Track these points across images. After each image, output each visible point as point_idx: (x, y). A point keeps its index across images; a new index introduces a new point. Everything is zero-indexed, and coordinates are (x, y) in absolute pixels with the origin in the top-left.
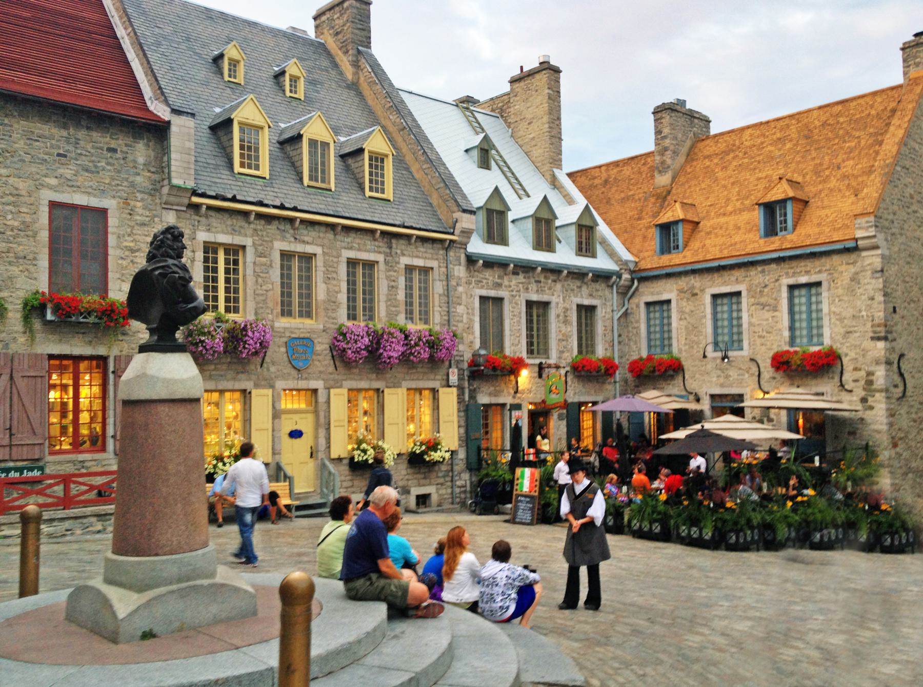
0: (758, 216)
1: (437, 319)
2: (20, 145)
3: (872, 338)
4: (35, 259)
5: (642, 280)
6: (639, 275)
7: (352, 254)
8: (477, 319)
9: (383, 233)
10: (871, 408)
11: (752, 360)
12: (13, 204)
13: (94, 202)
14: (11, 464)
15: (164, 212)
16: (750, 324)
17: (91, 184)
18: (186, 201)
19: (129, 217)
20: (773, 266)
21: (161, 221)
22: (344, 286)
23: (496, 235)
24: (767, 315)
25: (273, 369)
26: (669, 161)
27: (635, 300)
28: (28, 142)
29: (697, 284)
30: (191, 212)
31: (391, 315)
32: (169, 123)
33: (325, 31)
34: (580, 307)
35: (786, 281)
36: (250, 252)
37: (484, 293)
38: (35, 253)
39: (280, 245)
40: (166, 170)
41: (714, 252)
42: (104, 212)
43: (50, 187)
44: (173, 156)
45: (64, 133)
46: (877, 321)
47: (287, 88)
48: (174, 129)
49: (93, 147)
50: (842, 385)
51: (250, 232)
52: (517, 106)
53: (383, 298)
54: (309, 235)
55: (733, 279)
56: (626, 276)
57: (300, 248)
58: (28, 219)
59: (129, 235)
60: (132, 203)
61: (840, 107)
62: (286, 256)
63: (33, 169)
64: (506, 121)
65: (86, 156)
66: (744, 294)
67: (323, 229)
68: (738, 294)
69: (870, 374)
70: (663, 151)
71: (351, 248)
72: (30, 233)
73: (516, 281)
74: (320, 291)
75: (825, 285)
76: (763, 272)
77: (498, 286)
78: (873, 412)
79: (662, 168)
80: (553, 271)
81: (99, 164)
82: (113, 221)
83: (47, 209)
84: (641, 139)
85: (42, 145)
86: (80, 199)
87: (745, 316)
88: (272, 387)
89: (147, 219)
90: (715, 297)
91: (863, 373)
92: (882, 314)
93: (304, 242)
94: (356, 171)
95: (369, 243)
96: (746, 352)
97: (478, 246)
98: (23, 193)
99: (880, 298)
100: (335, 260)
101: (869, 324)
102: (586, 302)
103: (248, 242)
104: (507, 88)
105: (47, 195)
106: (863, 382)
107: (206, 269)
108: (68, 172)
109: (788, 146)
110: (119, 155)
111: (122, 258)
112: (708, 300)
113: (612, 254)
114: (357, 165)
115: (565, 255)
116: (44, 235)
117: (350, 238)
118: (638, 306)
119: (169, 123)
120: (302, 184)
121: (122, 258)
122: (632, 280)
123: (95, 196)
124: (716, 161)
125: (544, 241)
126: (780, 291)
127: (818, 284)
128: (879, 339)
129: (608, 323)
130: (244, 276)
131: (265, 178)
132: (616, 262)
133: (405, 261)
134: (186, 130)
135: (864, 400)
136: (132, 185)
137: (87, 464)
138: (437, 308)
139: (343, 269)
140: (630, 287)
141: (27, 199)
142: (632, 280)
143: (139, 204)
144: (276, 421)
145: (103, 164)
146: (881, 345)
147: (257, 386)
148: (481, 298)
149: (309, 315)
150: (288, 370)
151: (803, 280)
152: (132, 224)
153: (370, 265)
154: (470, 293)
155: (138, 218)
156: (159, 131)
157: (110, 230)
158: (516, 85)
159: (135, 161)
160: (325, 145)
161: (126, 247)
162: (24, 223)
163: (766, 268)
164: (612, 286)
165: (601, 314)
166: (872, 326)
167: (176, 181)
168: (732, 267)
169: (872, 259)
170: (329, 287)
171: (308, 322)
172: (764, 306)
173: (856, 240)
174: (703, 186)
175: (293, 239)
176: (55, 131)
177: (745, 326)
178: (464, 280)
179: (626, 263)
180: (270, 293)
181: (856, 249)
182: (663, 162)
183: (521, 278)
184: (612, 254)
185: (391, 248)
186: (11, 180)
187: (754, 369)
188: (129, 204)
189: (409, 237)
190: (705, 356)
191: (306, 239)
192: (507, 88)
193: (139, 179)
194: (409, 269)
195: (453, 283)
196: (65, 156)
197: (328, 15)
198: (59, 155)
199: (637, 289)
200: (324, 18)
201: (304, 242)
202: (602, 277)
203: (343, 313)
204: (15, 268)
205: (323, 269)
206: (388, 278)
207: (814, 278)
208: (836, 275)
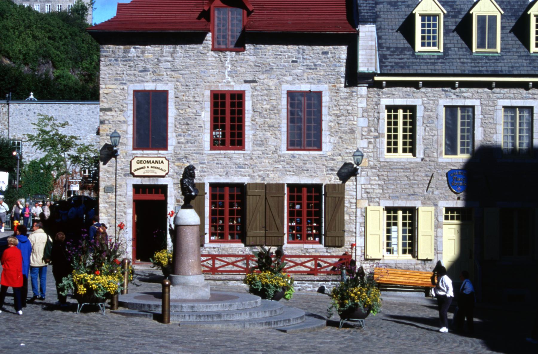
4: (279, 127)
7: (508, 103)
12: (267, 95)
13: (314, 88)
17: (312, 76)
19: (335, 94)
21: (357, 95)
25: (436, 192)
28: (275, 56)
38: (279, 123)
39: (445, 101)
42: (319, 94)
49: (313, 53)
54: (468, 92)
58: (275, 103)
59: (336, 106)
60: (338, 85)
62: (451, 110)
65: (309, 59)
72: (276, 111)
81: (317, 63)
82: (325, 99)
83: (286, 96)
85: (283, 57)
86: (305, 87)
88: (436, 205)
89: (348, 94)
100: (491, 108)
105: (287, 87)
107: (389, 123)
108: (298, 71)
110: (330, 55)
111: (331, 121)
116: (284, 113)
121: (331, 121)
123: (314, 84)
131: (439, 52)
134: (370, 34)
137: (309, 250)
141: (274, 91)
144: (439, 230)
145: (320, 63)
147: (424, 204)
155: (342, 94)
157: (323, 104)
160: (493, 19)
161: (334, 114)
162: (272, 106)
175: (454, 97)
188: (335, 86)
191: (465, 95)
196: (296, 62)
198: (293, 61)
201: (464, 97)
205: (481, 116)
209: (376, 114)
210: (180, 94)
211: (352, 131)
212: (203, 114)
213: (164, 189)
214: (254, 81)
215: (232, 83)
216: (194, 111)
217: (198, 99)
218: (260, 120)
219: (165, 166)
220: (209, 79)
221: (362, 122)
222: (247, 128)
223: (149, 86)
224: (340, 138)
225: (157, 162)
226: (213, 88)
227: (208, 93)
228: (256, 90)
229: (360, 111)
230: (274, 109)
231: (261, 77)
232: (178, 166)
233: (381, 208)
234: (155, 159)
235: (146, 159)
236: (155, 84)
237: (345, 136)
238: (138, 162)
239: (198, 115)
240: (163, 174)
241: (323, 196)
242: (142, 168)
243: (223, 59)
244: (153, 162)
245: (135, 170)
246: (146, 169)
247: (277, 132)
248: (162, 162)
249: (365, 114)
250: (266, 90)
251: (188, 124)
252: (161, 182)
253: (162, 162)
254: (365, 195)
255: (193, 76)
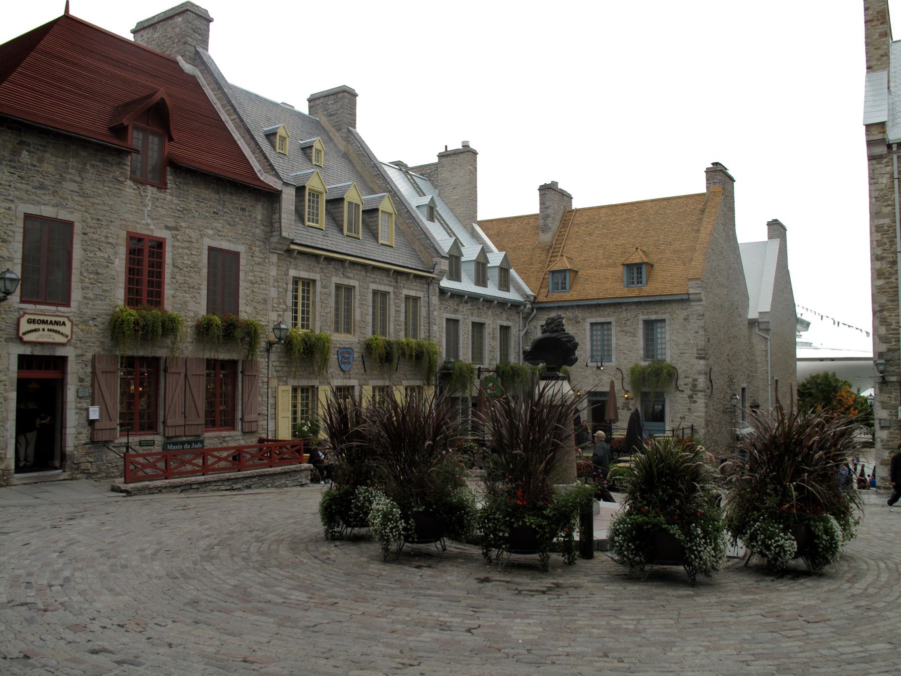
0: (621, 270)
1: (422, 337)
2: (193, 205)
3: (697, 358)
4: (199, 288)
5: (540, 309)
6: (538, 306)
8: (444, 335)
9: (396, 272)
10: (695, 402)
11: (618, 369)
12: (188, 248)
14: (184, 439)
15: (271, 255)
16: (617, 344)
18: (286, 248)
20: (634, 307)
22: (371, 309)
23: (455, 275)
24: (630, 339)
26: (550, 225)
27: (534, 323)
29: (580, 315)
30: (286, 255)
31: (397, 332)
32: (281, 192)
33: (320, 111)
34: (502, 327)
35: (642, 317)
36: (318, 284)
37: (449, 316)
39: (336, 280)
40: (277, 225)
41: (593, 294)
43: (208, 236)
44: (283, 215)
45: (217, 197)
46: (700, 347)
47: (314, 158)
48: (284, 196)
49: (233, 208)
50: (677, 387)
51: (318, 270)
52: (444, 174)
53: (392, 319)
55: (606, 313)
56: (529, 306)
57: (346, 282)
60: (253, 248)
61: (665, 202)
63: (200, 222)
64: (433, 184)
66: (613, 324)
67: (359, 268)
68: (610, 323)
69: (695, 380)
70: (546, 217)
71: (374, 282)
73: (465, 309)
74: (357, 315)
75: (667, 322)
76: (626, 310)
77: (456, 311)
78: (697, 405)
79: (545, 229)
80: (488, 301)
82: (243, 262)
83: (206, 252)
84: (531, 206)
86: (225, 245)
87: (614, 341)
90: (592, 324)
91: (690, 380)
92: (703, 343)
93: (348, 277)
94: (370, 224)
95: (385, 280)
96: (614, 363)
97: (445, 283)
98: (194, 240)
99: (702, 332)
101: (695, 349)
102: (505, 324)
103: (317, 277)
104: (436, 160)
105: (208, 242)
106: (690, 386)
108: (218, 225)
109: (634, 224)
110: (247, 214)
112: (588, 327)
113: (519, 289)
114: (371, 220)
115: (492, 290)
116: (205, 271)
117: (376, 276)
118: (535, 328)
119: (281, 192)
120: (343, 233)
122: (532, 309)
124: (583, 228)
125: (481, 280)
126: (637, 324)
127: (663, 321)
128: (701, 358)
129: (517, 339)
130: (314, 302)
132: (522, 295)
133: (405, 292)
135: (691, 397)
136: (254, 235)
138: (422, 327)
139: (370, 296)
140: (530, 314)
142: (532, 309)
143: (257, 249)
146: (702, 362)
147: (321, 383)
148: (447, 319)
149: (348, 331)
150: (339, 372)
151: (653, 317)
152: (253, 263)
153: (385, 294)
154: (441, 315)
156: (272, 197)
158: (444, 159)
159: (256, 218)
162: (193, 262)
163: (629, 308)
164: (519, 313)
165: (514, 331)
166: (697, 350)
167: (285, 234)
168: (605, 305)
169: (696, 308)
170: (362, 311)
171: (349, 336)
172: (626, 332)
173: (688, 294)
174: (576, 245)
176: (212, 195)
177: (613, 346)
178: (437, 307)
179: (528, 296)
180: (329, 315)
181: (688, 300)
182: (546, 225)
183: (469, 306)
184: (519, 289)
185: (397, 282)
186: (187, 231)
187: (619, 375)
189: (408, 274)
190: (587, 366)
191: (350, 275)
192: (436, 160)
193: (257, 231)
194: (407, 298)
195: (432, 309)
196: (217, 213)
197: (322, 100)
198: (214, 213)
199: (535, 316)
200: (318, 102)
202: (515, 306)
203: (370, 329)
204: (187, 295)
206: (395, 304)
207: (660, 317)
208: (675, 316)
209: (285, 286)
210: (89, 230)
211: (265, 301)
212: (117, 262)
213: (62, 361)
214: (177, 229)
215: (152, 227)
216: (106, 256)
217: (111, 240)
218: (180, 279)
219: (66, 330)
220: (126, 216)
221: (273, 293)
222: (166, 287)
223: (48, 211)
224: (255, 308)
225: (57, 323)
226: (130, 229)
227: (124, 234)
228: (178, 240)
229: (272, 280)
230: (195, 266)
231: (183, 224)
232: (82, 330)
233: (290, 388)
234: (54, 319)
235: (42, 318)
236: (55, 209)
237: (259, 307)
238: (30, 321)
239: (110, 261)
240: (63, 340)
241: (240, 375)
242: (35, 330)
243: (143, 194)
244: (51, 322)
245: (25, 334)
246: (41, 332)
247: (196, 295)
248: (64, 324)
249: (276, 284)
250: (188, 242)
251: (97, 273)
252: (60, 352)
253: (64, 324)
254: (275, 374)
255: (107, 208)
